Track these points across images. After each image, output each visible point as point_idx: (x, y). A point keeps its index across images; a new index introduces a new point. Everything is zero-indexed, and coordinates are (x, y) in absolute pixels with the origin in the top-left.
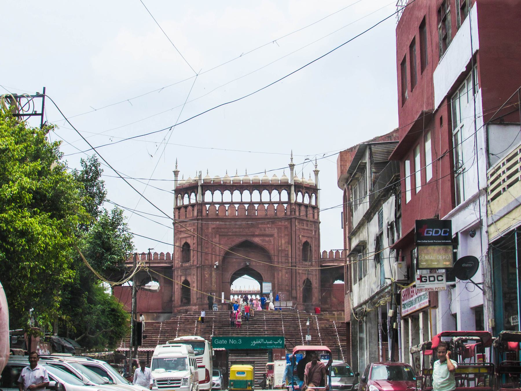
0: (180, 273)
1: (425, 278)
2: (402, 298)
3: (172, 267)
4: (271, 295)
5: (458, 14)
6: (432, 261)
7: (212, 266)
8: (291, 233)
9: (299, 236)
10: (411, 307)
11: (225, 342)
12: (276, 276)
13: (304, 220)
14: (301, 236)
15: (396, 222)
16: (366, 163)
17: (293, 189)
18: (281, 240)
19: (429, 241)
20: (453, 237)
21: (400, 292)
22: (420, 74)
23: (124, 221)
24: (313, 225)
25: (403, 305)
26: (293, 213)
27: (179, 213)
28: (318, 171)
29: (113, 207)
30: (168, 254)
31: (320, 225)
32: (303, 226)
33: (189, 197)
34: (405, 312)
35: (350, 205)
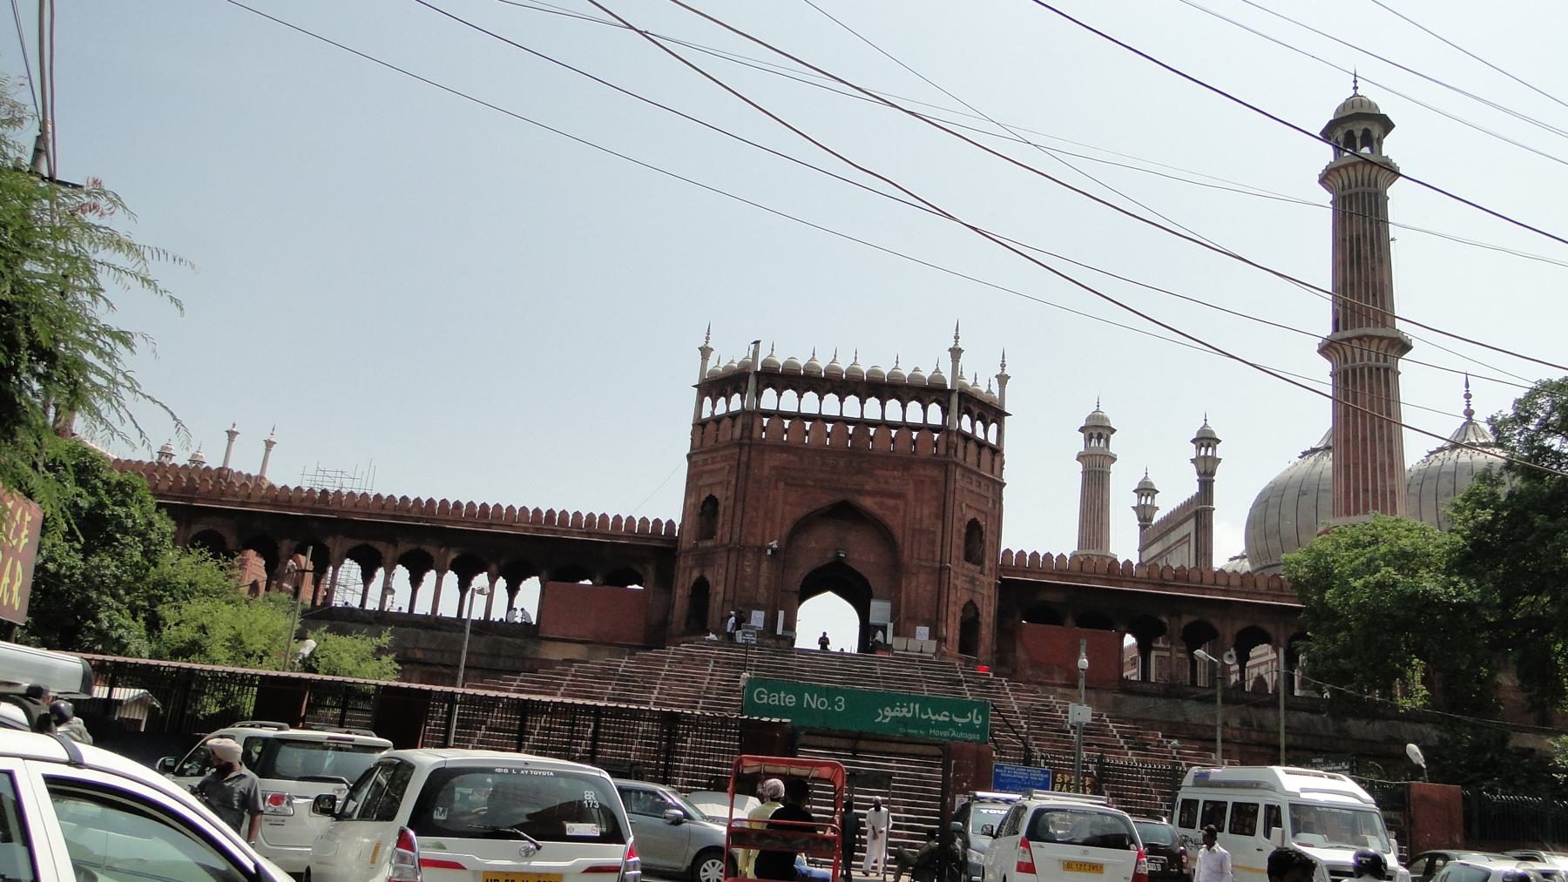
0: (690, 563)
3: (676, 548)
4: (890, 626)
7: (761, 549)
9: (961, 504)
11: (790, 700)
12: (903, 586)
13: (971, 471)
14: (964, 505)
17: (955, 400)
18: (922, 510)
24: (991, 488)
26: (953, 451)
27: (703, 433)
30: (670, 523)
31: (1005, 490)
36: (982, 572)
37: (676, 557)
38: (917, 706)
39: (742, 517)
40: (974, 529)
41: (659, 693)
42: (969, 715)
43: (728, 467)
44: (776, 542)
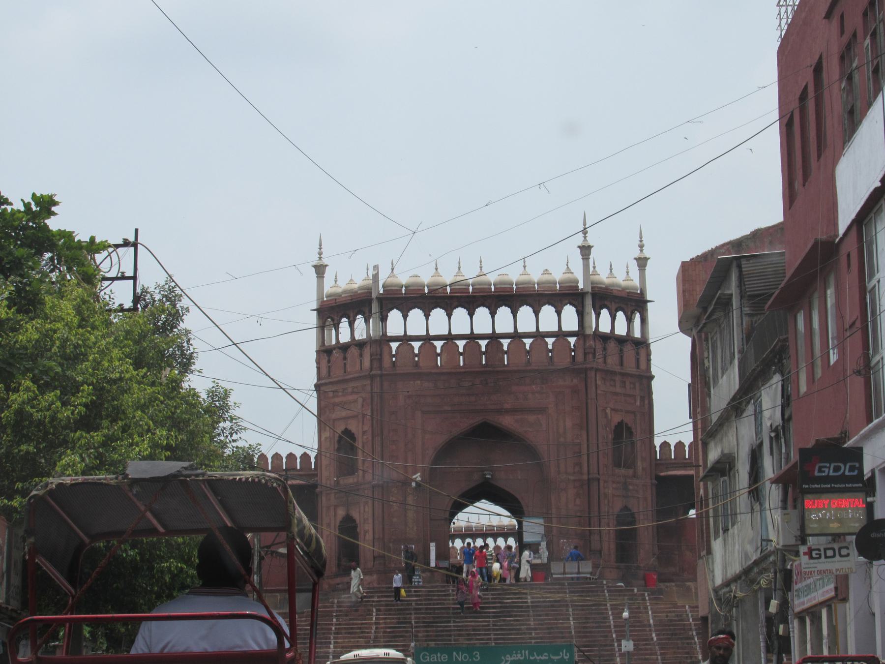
1: (817, 552)
2: (795, 577)
3: (315, 486)
4: (544, 545)
5: (869, 79)
6: (830, 521)
7: (406, 482)
8: (587, 404)
9: (604, 410)
10: (809, 597)
13: (613, 373)
14: (608, 411)
15: (783, 427)
16: (732, 295)
17: (589, 301)
19: (823, 486)
20: (865, 478)
21: (792, 565)
22: (816, 159)
23: (234, 412)
24: (637, 385)
25: (797, 591)
26: (591, 356)
27: (329, 361)
28: (646, 259)
29: (210, 385)
30: (305, 457)
32: (615, 386)
33: (351, 325)
34: (799, 603)
35: (705, 371)
36: (635, 475)
37: (317, 495)
38: (527, 652)
39: (382, 451)
40: (621, 431)
41: (335, 647)
42: (561, 653)
43: (360, 400)
44: (419, 474)
